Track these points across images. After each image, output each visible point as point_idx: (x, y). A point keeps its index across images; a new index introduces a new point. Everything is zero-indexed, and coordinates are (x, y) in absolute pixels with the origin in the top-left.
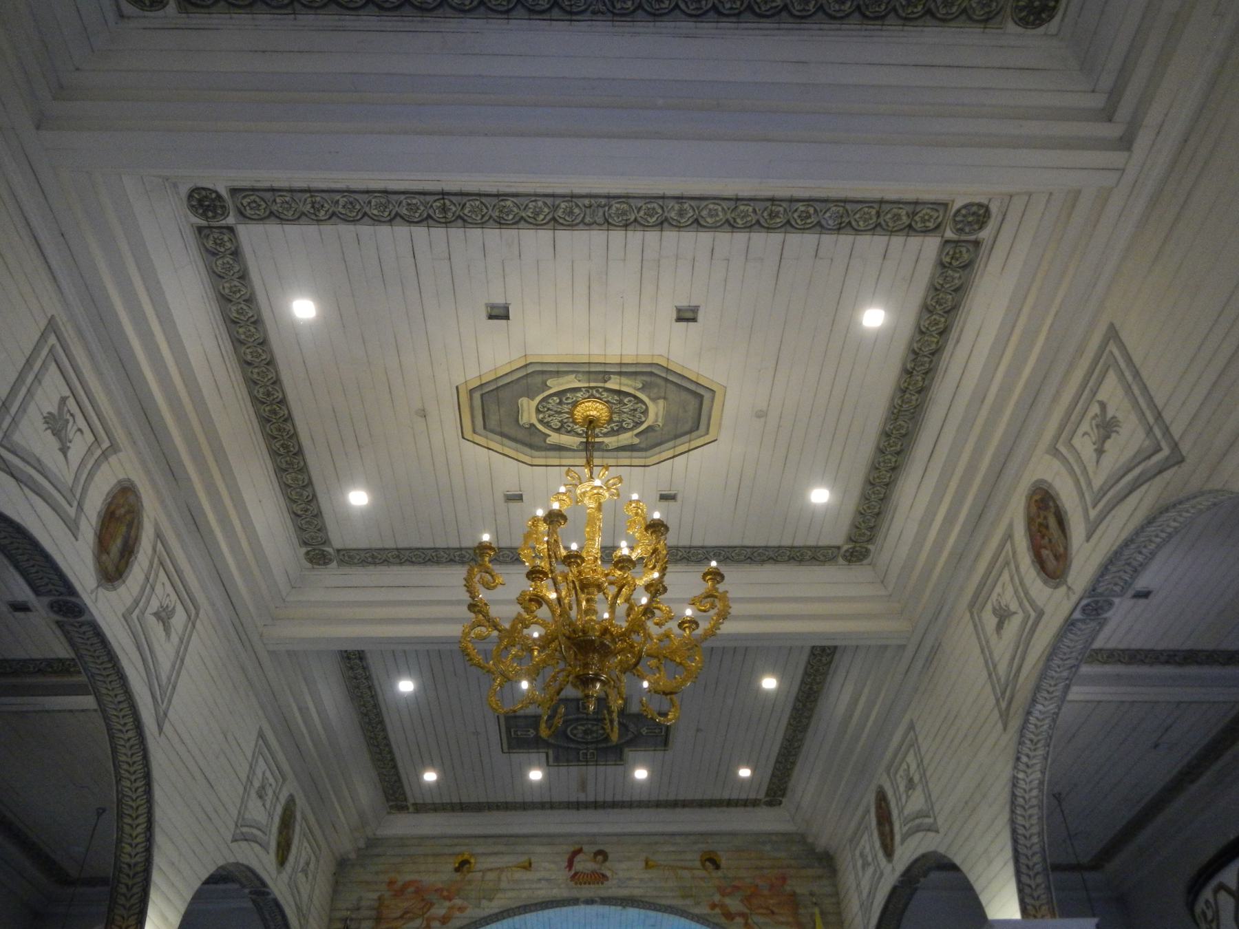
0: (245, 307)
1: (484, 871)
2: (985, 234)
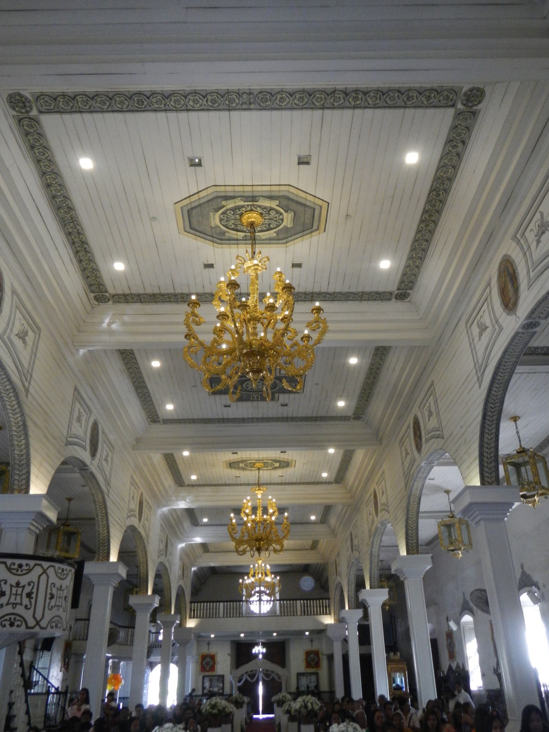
0: (412, 264)
2: (92, 295)
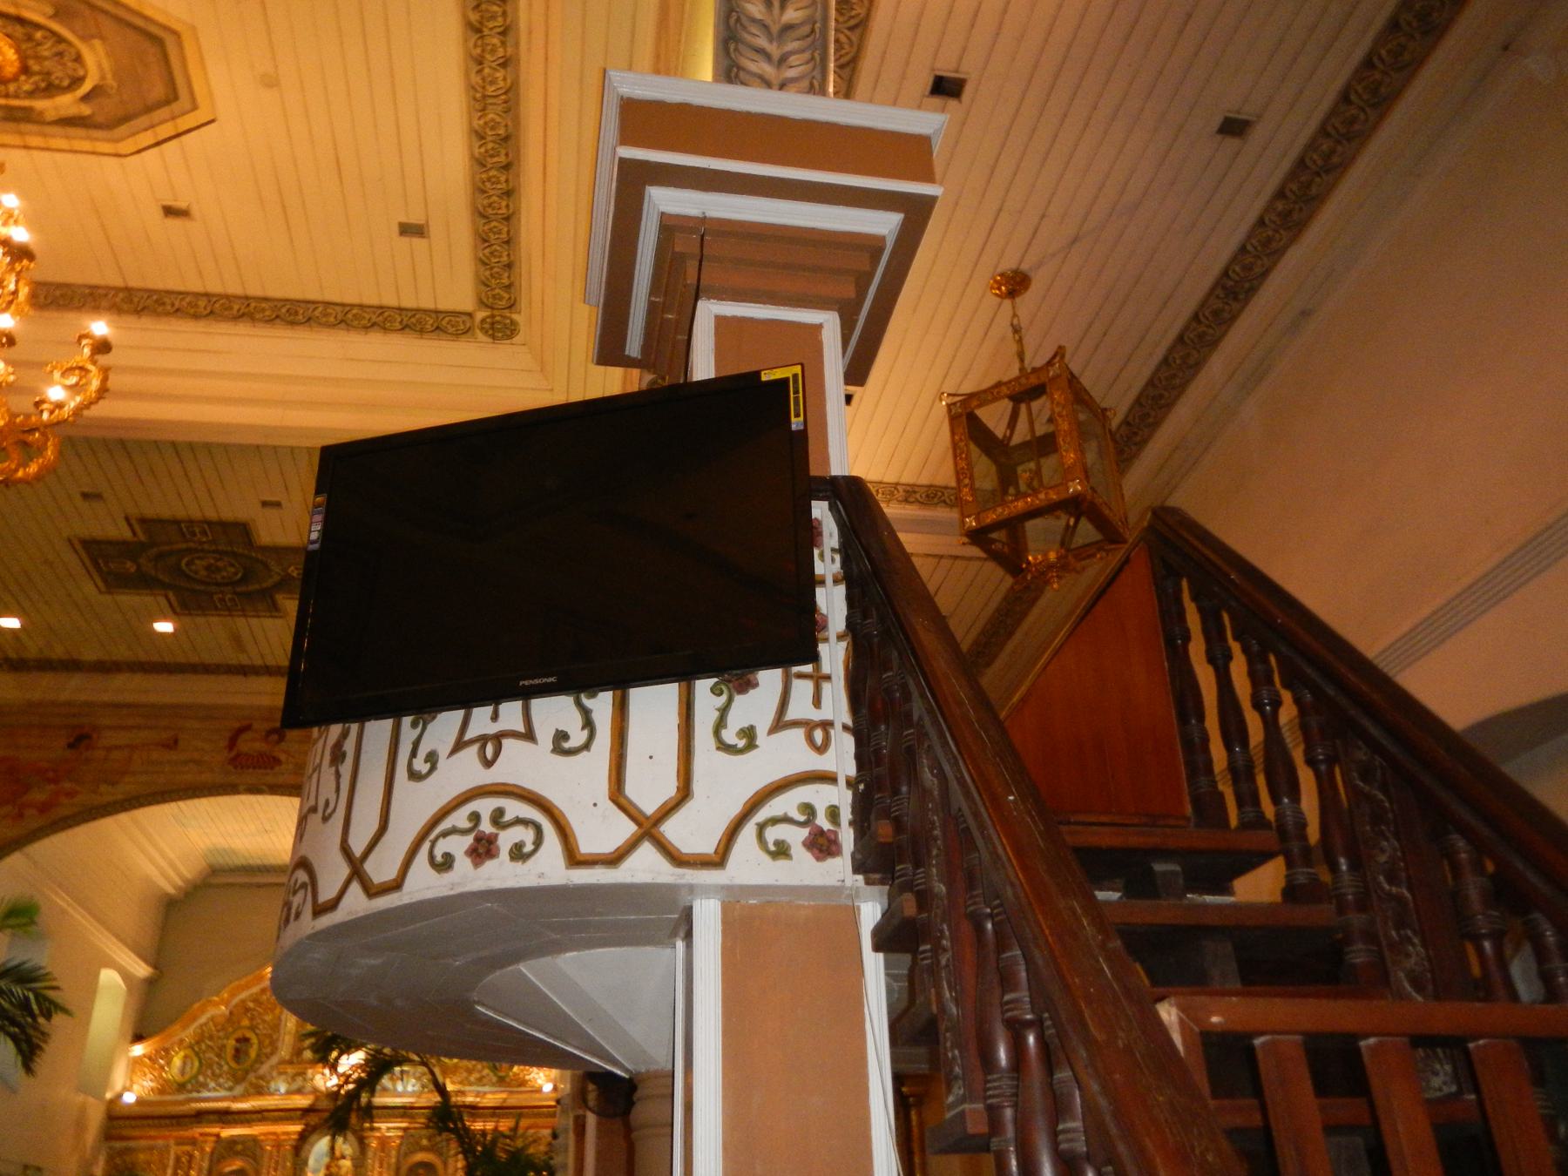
1: (109, 749)
